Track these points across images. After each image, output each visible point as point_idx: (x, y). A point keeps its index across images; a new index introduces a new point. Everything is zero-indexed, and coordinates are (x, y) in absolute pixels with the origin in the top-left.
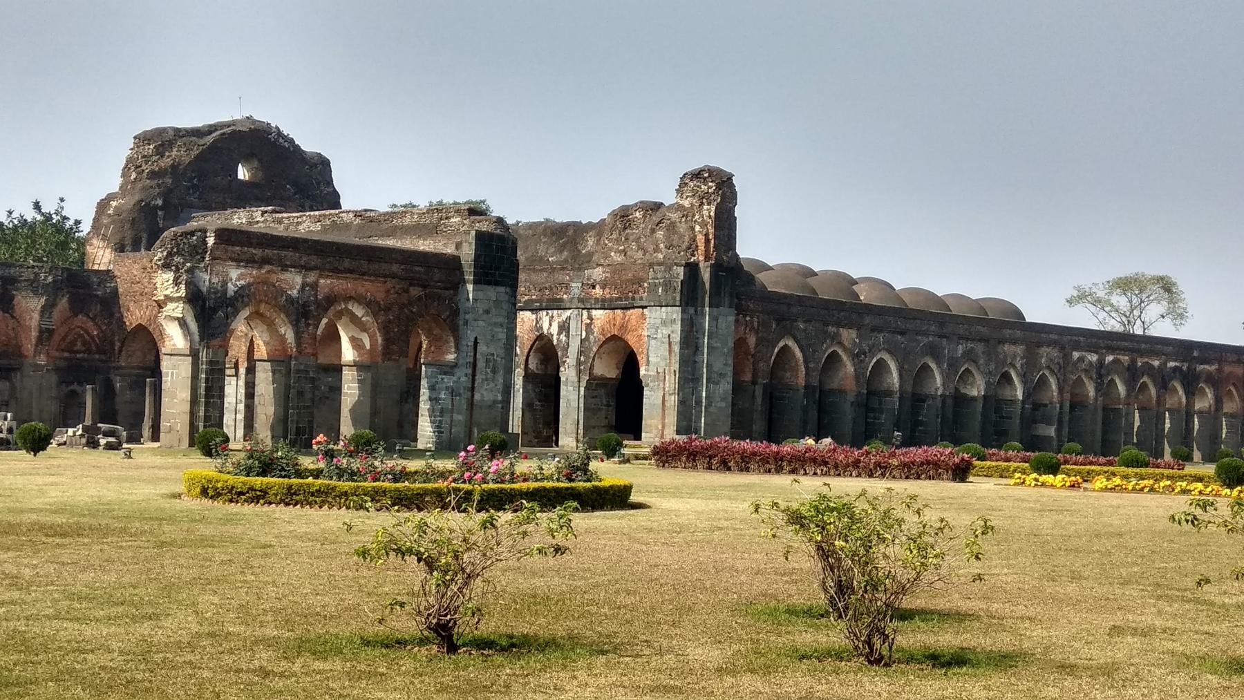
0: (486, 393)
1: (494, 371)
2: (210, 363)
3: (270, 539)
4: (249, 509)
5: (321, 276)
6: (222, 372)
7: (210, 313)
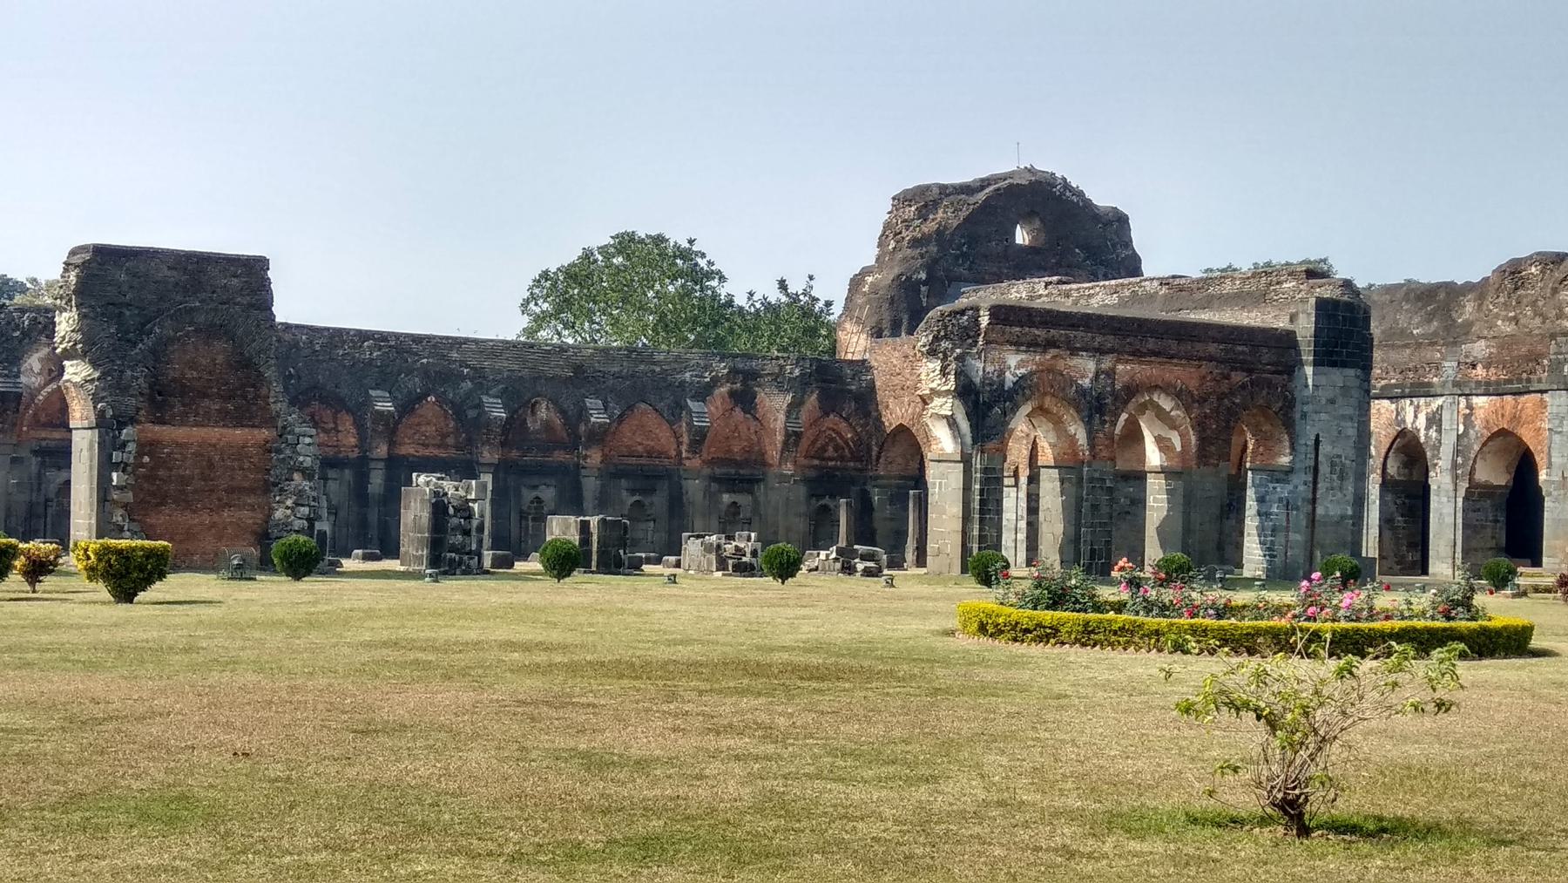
0: (1331, 506)
1: (1342, 478)
2: (985, 470)
3: (1064, 687)
4: (1036, 650)
5: (1119, 361)
6: (999, 481)
7: (985, 409)
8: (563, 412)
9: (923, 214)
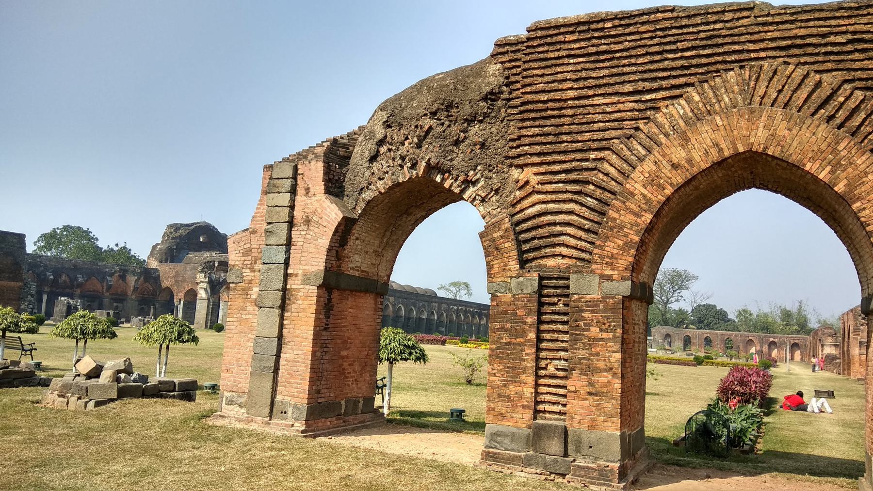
8: (70, 278)
9: (176, 231)
